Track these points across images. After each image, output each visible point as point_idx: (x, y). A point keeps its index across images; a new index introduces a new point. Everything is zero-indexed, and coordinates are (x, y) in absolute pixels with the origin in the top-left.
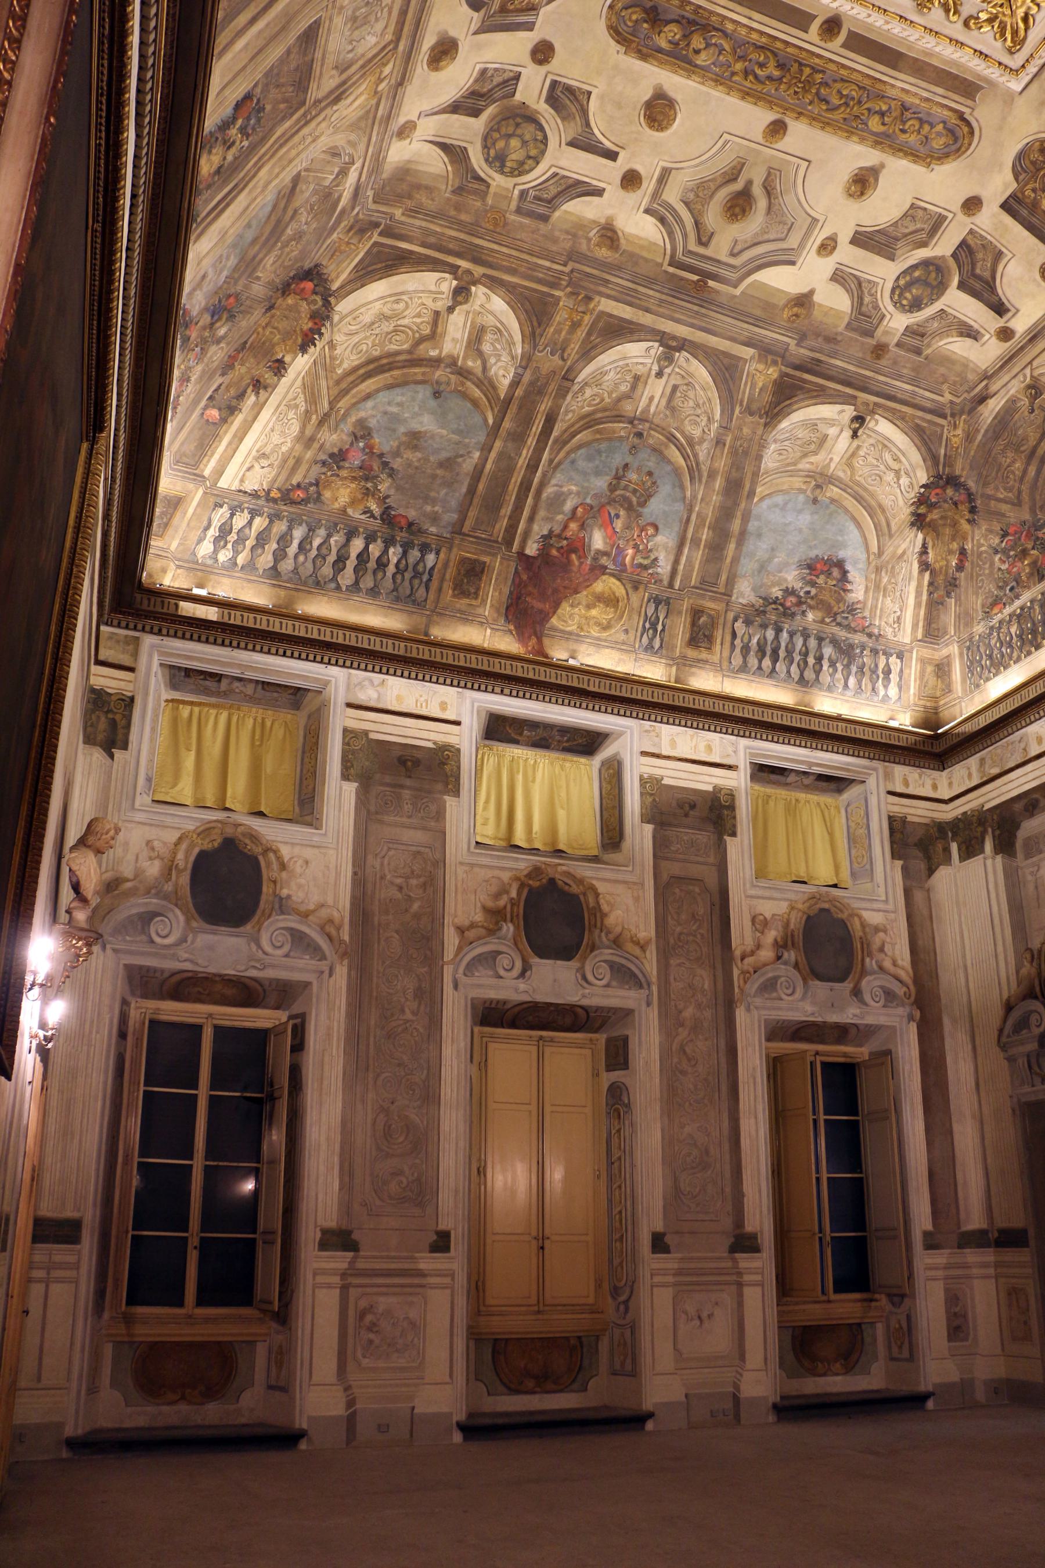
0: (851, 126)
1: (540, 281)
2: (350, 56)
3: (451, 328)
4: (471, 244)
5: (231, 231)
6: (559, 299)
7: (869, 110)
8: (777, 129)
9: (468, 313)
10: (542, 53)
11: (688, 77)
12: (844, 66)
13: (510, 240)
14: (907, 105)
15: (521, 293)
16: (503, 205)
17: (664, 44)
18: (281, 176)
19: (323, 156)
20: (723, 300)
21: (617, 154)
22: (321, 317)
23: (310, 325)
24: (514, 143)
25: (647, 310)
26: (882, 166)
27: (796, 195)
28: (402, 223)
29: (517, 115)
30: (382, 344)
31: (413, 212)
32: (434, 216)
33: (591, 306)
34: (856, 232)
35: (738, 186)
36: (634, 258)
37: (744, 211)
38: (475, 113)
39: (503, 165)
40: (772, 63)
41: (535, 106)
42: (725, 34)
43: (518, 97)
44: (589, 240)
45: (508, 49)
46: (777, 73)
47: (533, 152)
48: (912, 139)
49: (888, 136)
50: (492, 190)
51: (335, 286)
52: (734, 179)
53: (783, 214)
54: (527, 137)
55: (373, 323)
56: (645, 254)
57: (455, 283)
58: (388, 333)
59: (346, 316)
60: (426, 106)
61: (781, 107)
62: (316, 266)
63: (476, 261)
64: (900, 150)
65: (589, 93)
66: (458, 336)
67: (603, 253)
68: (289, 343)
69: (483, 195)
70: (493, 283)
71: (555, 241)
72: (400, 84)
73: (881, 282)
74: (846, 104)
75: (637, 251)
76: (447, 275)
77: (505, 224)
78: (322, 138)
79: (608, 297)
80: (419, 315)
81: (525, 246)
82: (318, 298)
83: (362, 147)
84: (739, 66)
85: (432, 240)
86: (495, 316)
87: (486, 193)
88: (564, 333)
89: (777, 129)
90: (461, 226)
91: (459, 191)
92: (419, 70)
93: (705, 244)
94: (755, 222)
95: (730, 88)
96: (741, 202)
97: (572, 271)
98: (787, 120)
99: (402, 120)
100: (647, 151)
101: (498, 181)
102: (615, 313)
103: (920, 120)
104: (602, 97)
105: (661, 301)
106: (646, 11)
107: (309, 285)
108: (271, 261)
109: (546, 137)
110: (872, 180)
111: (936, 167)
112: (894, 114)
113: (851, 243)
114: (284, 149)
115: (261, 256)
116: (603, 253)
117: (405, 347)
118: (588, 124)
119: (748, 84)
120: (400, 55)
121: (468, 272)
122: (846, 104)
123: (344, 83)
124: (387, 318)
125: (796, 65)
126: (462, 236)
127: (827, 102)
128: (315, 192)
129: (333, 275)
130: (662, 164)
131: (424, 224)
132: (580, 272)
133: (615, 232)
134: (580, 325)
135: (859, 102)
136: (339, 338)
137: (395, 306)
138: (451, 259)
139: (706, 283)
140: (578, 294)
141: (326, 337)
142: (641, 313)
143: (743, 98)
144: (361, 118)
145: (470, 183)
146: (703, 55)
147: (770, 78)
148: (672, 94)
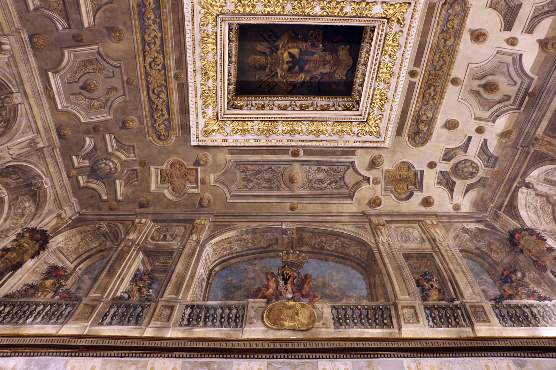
0: (452, 52)
1: (526, 158)
2: (419, 239)
3: (544, 190)
4: (506, 182)
5: (470, 279)
6: (535, 151)
7: (444, 47)
8: (455, 82)
9: (537, 184)
10: (432, 165)
11: (437, 118)
12: (427, 64)
13: (506, 169)
14: (441, 31)
15: (531, 164)
16: (490, 172)
17: (426, 128)
18: (458, 257)
19: (456, 241)
20: (540, 83)
21: (469, 137)
22: (532, 232)
23: (534, 236)
24: (466, 170)
25: (544, 115)
26: (470, 30)
27: (485, 65)
28: (496, 204)
29: (455, 170)
30: (548, 214)
31: (492, 200)
32: (494, 194)
33: (540, 137)
34: (504, 30)
35: (481, 90)
36: (517, 123)
37: (493, 85)
38: (454, 183)
39: (475, 173)
40: (429, 91)
41: (452, 165)
42: (420, 109)
43: (448, 170)
44: (507, 142)
45: (430, 178)
46: (432, 88)
47: (469, 164)
48: (456, 22)
49: (455, 34)
50: (484, 176)
51: (519, 226)
52: (478, 93)
53: (495, 68)
54: (463, 166)
55: (538, 216)
56: (514, 120)
57: (523, 187)
58: (543, 212)
59: (533, 224)
60: (448, 202)
61: (445, 83)
62: (509, 232)
63: (514, 180)
64: (462, 25)
65: (446, 148)
66: (548, 188)
67: (513, 136)
68: (540, 244)
69: (486, 179)
70: (525, 174)
71: (507, 154)
72: (436, 215)
73: (535, 5)
74: (442, 57)
75: (513, 123)
76: (520, 190)
77: (499, 171)
78: (449, 243)
79: (536, 131)
80: (537, 201)
81: (509, 164)
82: (523, 232)
83: (459, 226)
84: (431, 102)
85: (504, 194)
86: (541, 174)
87: (485, 178)
88: (553, 148)
89: (455, 82)
90: (499, 185)
91: (484, 186)
92: (433, 209)
93: (510, 97)
94: (500, 79)
95: (439, 104)
96: (488, 87)
97: (522, 146)
98: (451, 78)
99: (452, 210)
100: (468, 126)
101: (480, 174)
102: (544, 128)
103: (447, 22)
104: (447, 144)
105: (539, 110)
106: (416, 135)
107: (517, 235)
108: (496, 256)
109: (463, 160)
110: (477, 33)
111: (470, 4)
112: (445, 35)
113: (510, 30)
114: (447, 259)
115: (491, 261)
116: (513, 136)
117: (550, 207)
118: (458, 148)
119: (437, 98)
120: (425, 219)
121: (519, 183)
122: (442, 57)
123: (428, 239)
124: (536, 211)
125: (429, 82)
126: (503, 185)
127: (442, 65)
128: (471, 241)
129: (515, 227)
130: (473, 120)
131: (497, 197)
132: (522, 143)
133: (504, 132)
134: (549, 142)
135: (441, 52)
136: (542, 228)
137: (531, 208)
138: (513, 189)
139: (531, 92)
140: (533, 144)
141: (541, 232)
142: (545, 117)
143: (443, 98)
144: (446, 229)
145: (482, 182)
146: (429, 115)
147: (434, 90)
148: (444, 123)
